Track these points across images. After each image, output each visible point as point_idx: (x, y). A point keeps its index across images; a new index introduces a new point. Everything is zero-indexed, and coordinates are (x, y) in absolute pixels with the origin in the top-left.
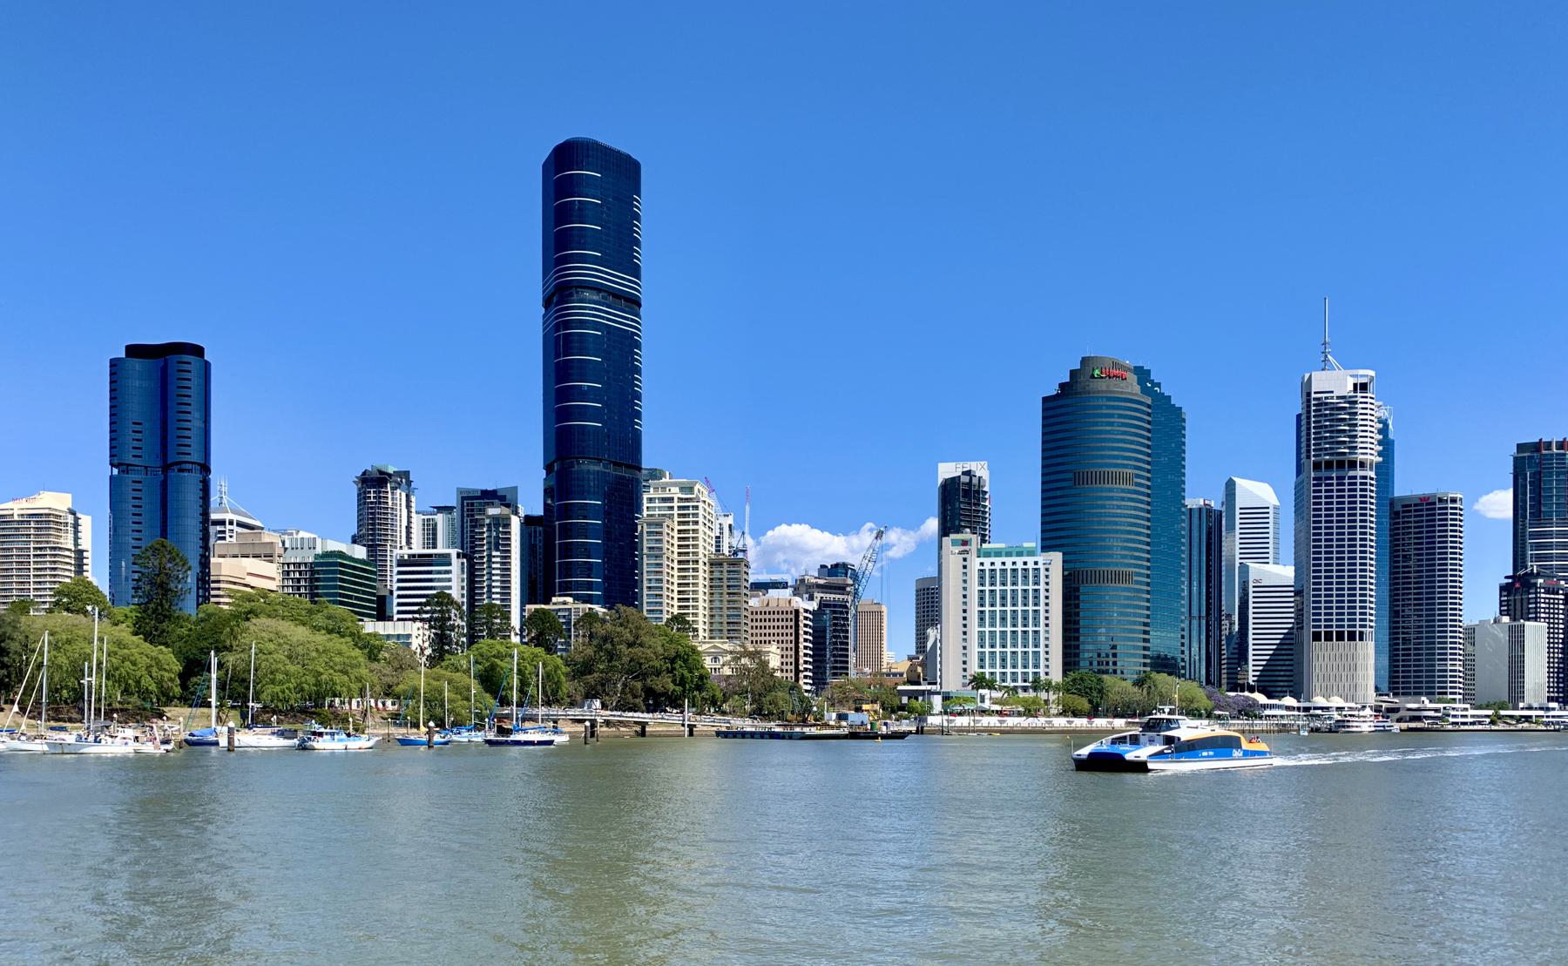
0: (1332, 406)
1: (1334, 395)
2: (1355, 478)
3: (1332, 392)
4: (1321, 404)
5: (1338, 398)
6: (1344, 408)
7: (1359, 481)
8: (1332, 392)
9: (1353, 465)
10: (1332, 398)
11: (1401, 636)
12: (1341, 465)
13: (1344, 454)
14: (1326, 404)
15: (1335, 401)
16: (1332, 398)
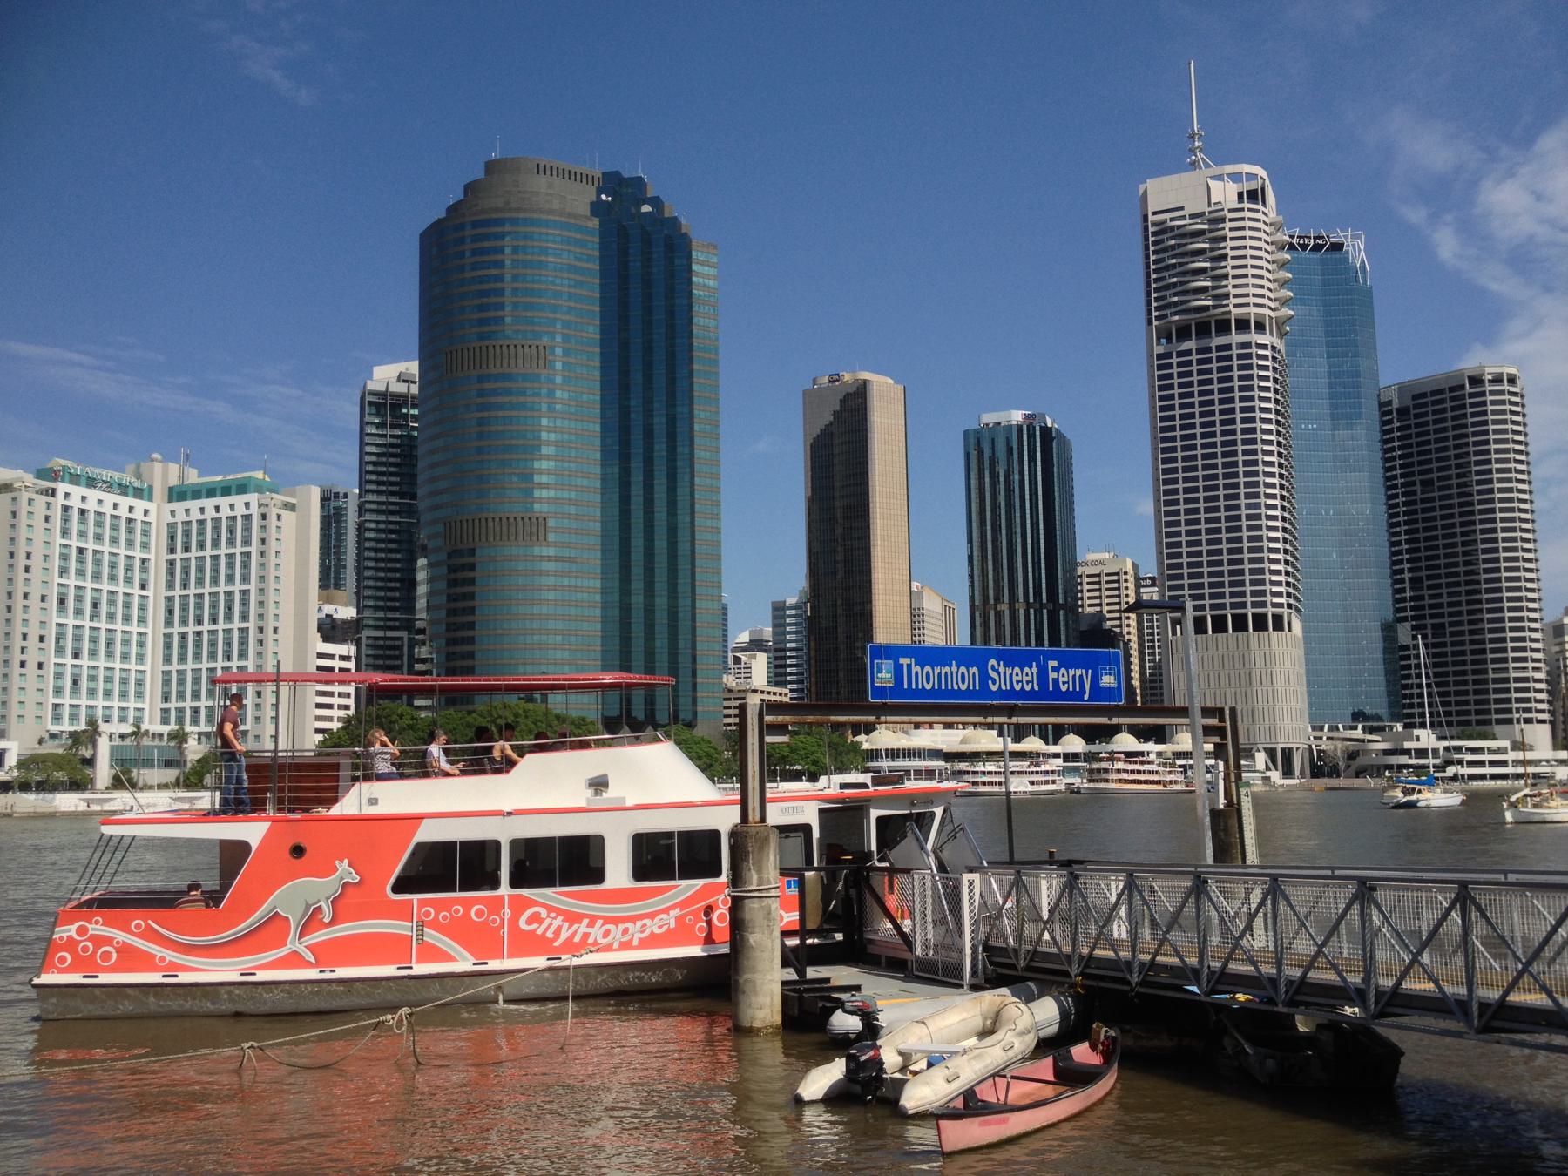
0: (1176, 232)
1: (1186, 212)
2: (1228, 347)
3: (1182, 208)
4: (1163, 230)
5: (1192, 216)
6: (1202, 233)
7: (1235, 352)
8: (1182, 208)
9: (1223, 327)
10: (1183, 218)
11: (1429, 622)
12: (1203, 330)
13: (1206, 308)
14: (1172, 228)
15: (1187, 221)
16: (1183, 218)
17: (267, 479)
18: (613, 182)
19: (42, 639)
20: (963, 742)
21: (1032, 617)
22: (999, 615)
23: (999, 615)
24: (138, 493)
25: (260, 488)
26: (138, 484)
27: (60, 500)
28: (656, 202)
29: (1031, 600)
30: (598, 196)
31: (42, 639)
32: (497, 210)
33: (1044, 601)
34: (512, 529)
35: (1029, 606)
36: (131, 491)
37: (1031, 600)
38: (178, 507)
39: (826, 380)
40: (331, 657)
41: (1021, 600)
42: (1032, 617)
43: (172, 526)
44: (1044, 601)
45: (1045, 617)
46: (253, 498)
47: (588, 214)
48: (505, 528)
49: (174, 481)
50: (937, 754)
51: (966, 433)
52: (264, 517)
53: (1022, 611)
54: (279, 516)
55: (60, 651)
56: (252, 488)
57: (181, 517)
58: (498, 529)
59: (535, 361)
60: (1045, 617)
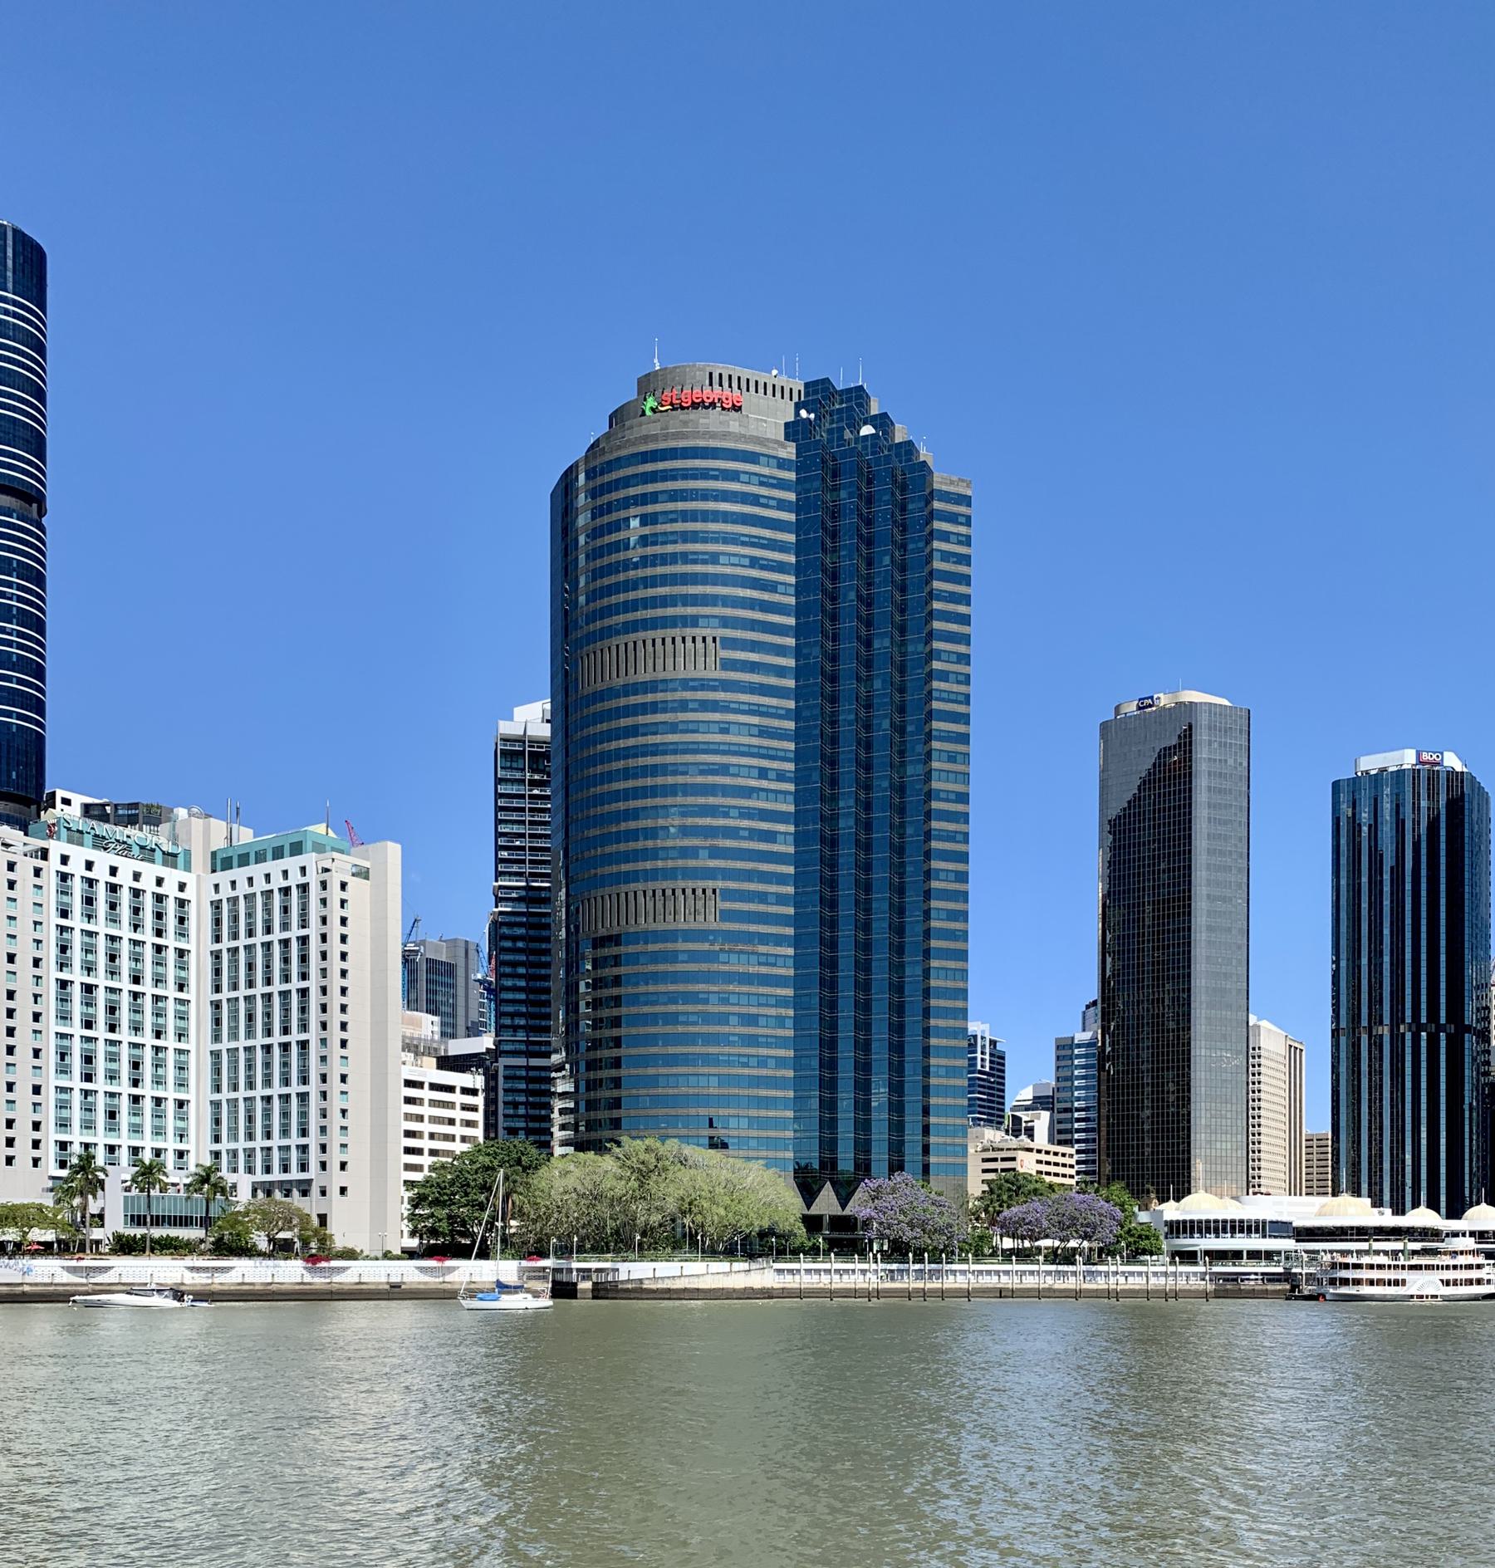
17: (331, 834)
18: (818, 393)
19: (37, 1053)
20: (1320, 1214)
21: (1424, 1044)
22: (1376, 1043)
23: (1376, 1043)
24: (170, 859)
25: (319, 848)
26: (168, 847)
27: (54, 862)
28: (883, 422)
29: (1424, 1020)
30: (797, 414)
31: (37, 1053)
32: (646, 439)
33: (1443, 1021)
34: (670, 905)
35: (1417, 1028)
36: (158, 855)
37: (1424, 1020)
38: (224, 878)
39: (1133, 707)
40: (450, 1089)
41: (1408, 1020)
42: (1424, 1044)
43: (216, 906)
44: (1443, 1021)
45: (1443, 1044)
46: (309, 859)
47: (782, 438)
48: (660, 905)
49: (219, 843)
50: (1280, 1228)
51: (1336, 785)
52: (324, 885)
53: (1408, 1036)
54: (343, 886)
55: (64, 1070)
56: (308, 845)
57: (226, 892)
58: (650, 905)
59: (701, 660)
60: (1443, 1044)
